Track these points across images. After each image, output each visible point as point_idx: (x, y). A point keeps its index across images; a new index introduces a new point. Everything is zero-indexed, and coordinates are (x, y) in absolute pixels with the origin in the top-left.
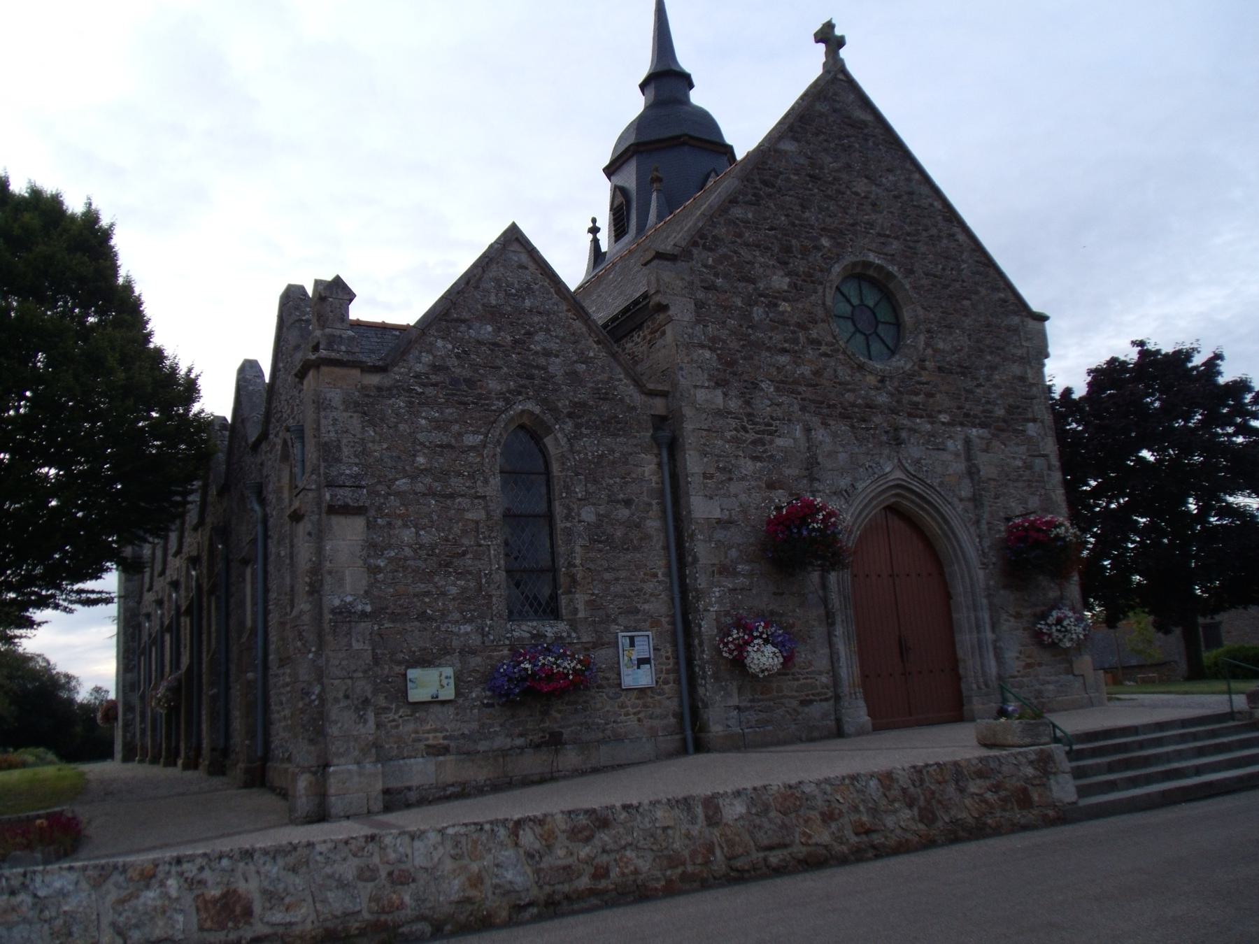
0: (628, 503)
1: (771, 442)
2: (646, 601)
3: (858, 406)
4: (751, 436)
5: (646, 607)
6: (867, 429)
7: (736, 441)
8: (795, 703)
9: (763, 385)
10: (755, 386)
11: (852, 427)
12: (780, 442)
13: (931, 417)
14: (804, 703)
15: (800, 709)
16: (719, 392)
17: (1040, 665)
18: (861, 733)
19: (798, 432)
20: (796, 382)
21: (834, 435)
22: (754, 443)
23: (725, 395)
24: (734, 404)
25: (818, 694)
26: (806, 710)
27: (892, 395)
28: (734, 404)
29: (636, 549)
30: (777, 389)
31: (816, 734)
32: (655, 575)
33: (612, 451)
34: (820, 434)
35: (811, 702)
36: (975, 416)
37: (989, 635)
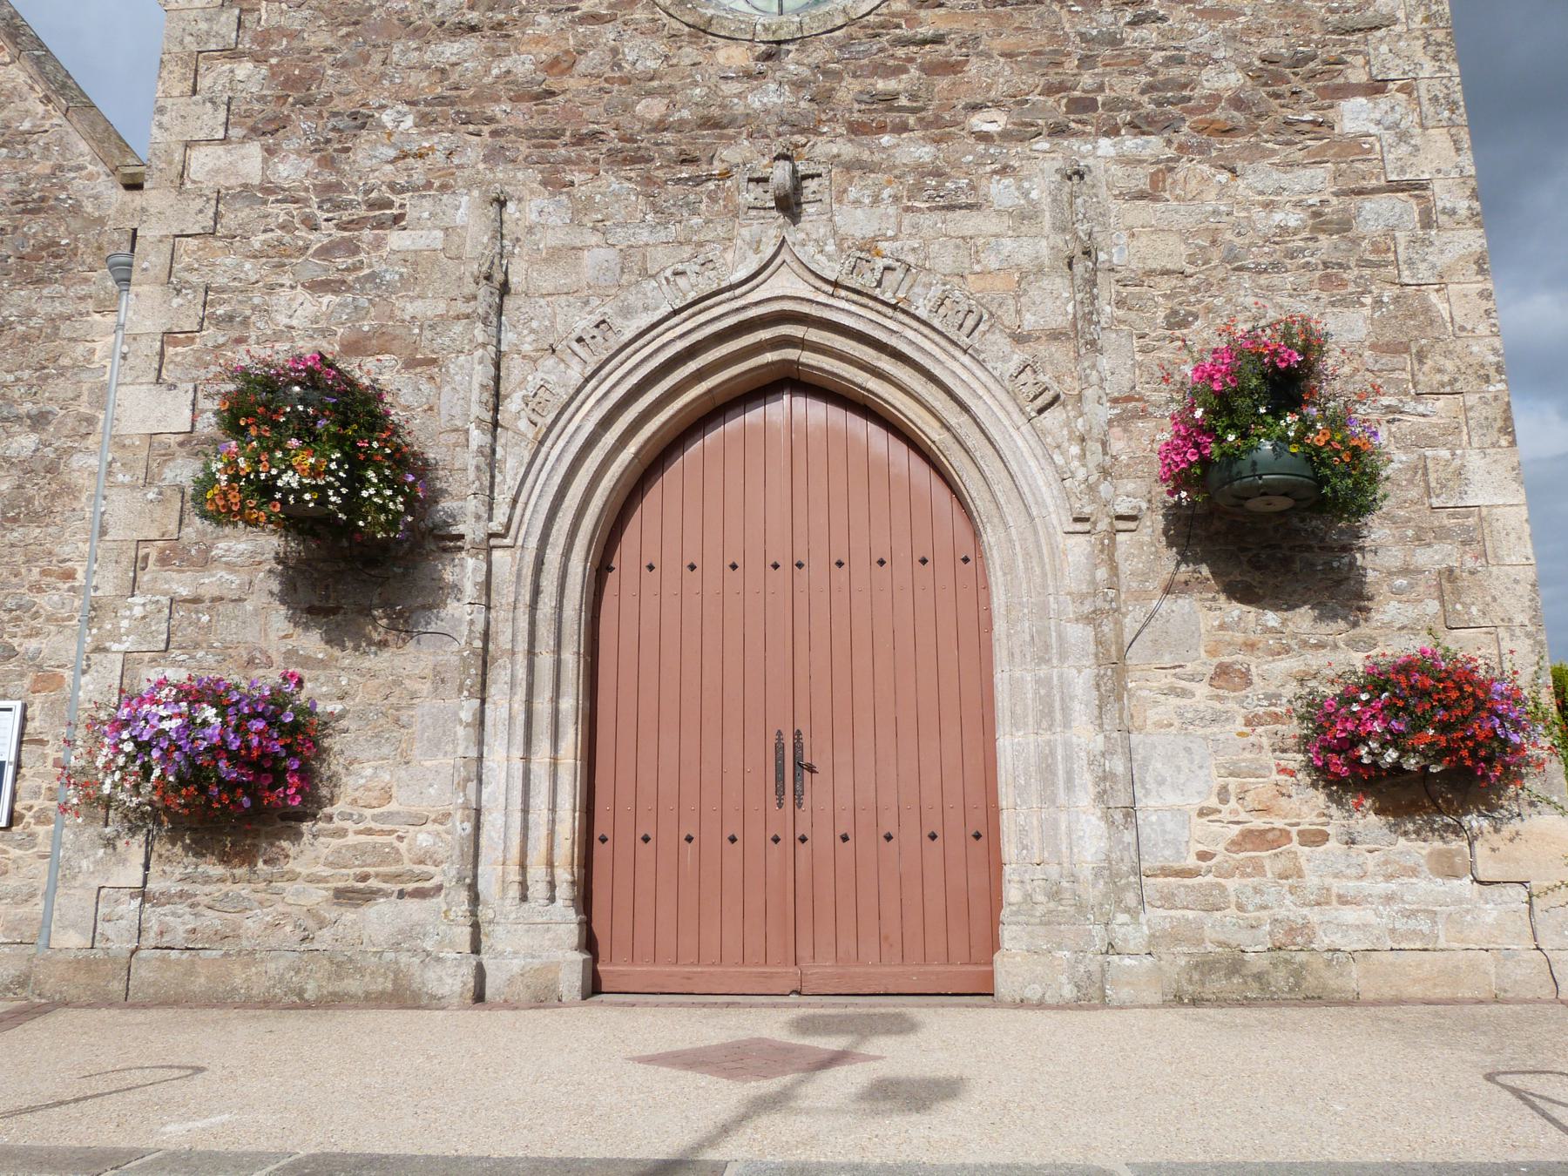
0: (39, 421)
1: (378, 244)
2: (35, 633)
3: (680, 127)
4: (329, 233)
5: (33, 644)
6: (698, 181)
7: (278, 256)
8: (318, 896)
9: (387, 118)
10: (361, 121)
11: (648, 180)
12: (396, 240)
13: (939, 128)
14: (344, 896)
15: (331, 913)
16: (254, 149)
17: (1316, 838)
18: (544, 998)
19: (466, 210)
20: (486, 95)
21: (581, 209)
22: (326, 252)
23: (270, 151)
24: (292, 169)
25: (397, 877)
26: (349, 915)
27: (799, 85)
28: (292, 169)
29: (35, 518)
30: (425, 120)
31: (353, 985)
32: (69, 575)
33: (31, 314)
34: (534, 208)
35: (370, 896)
36: (1114, 105)
37: (1084, 735)
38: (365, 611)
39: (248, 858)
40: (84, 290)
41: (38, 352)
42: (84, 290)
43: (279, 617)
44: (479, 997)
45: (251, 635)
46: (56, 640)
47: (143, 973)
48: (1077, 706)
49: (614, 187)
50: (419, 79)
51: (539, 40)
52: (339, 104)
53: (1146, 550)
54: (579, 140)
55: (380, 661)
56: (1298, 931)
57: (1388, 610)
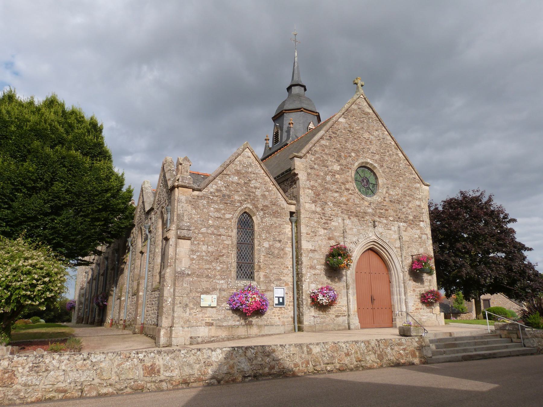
0: (280, 241)
1: (330, 223)
2: (284, 276)
3: (361, 213)
4: (324, 221)
5: (284, 278)
6: (364, 221)
7: (319, 222)
8: (334, 316)
9: (329, 203)
10: (326, 203)
11: (359, 220)
12: (333, 223)
13: (386, 218)
14: (337, 316)
15: (335, 319)
16: (313, 205)
17: (421, 309)
18: (356, 329)
19: (340, 220)
20: (340, 203)
21: (353, 222)
22: (324, 223)
23: (316, 206)
24: (319, 209)
25: (342, 314)
26: (338, 319)
27: (373, 209)
28: (319, 209)
29: (282, 258)
30: (334, 205)
31: (340, 328)
32: (288, 267)
33: (276, 223)
34: (347, 221)
35: (339, 316)
36: (402, 219)
37: (403, 297)
38: (335, 277)
39: (325, 311)
40: (284, 220)
41: (278, 230)
42: (284, 220)
43: (325, 278)
44: (349, 329)
45: (322, 280)
46: (288, 278)
47: (317, 327)
48: (351, 287)
49: (355, 220)
50: (332, 198)
51: (346, 196)
52: (323, 200)
53: (407, 276)
54: (351, 212)
55: (337, 284)
56: (421, 319)
57: (426, 284)
